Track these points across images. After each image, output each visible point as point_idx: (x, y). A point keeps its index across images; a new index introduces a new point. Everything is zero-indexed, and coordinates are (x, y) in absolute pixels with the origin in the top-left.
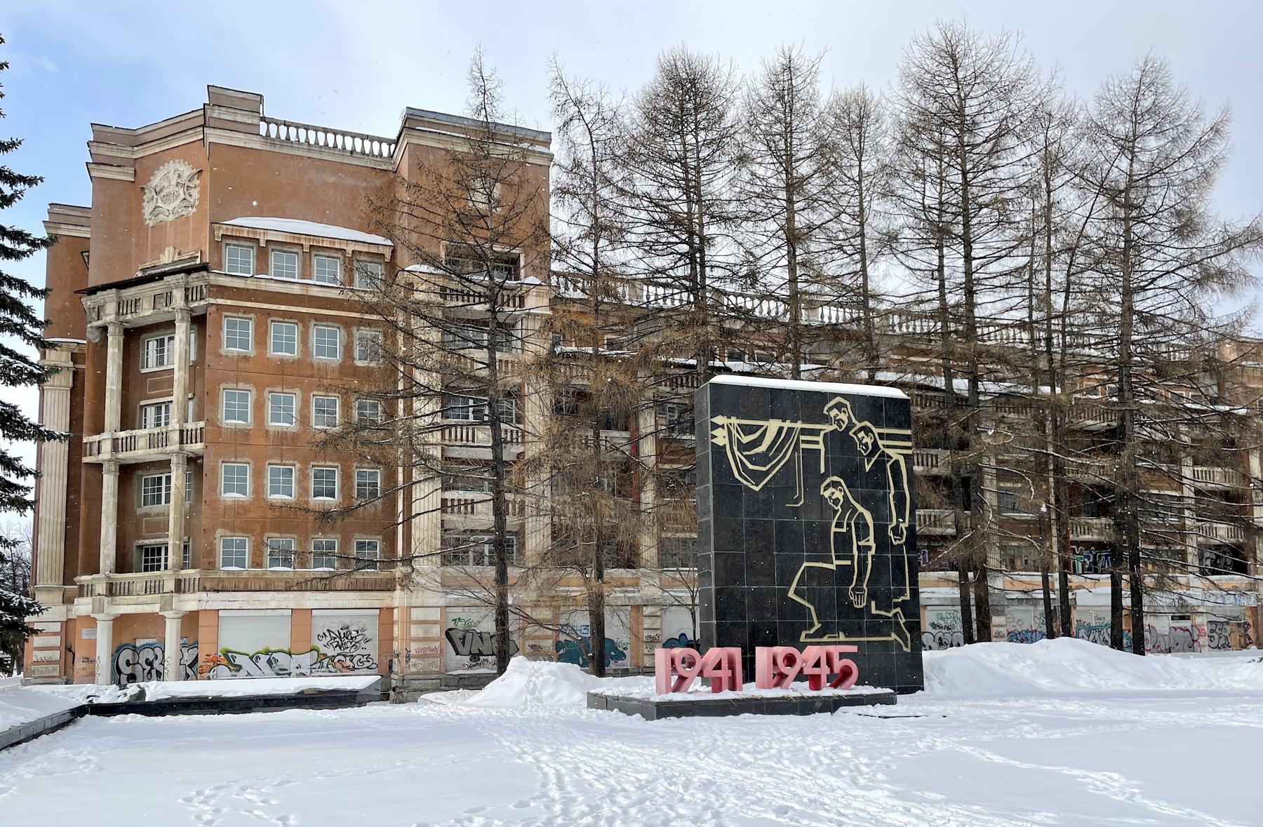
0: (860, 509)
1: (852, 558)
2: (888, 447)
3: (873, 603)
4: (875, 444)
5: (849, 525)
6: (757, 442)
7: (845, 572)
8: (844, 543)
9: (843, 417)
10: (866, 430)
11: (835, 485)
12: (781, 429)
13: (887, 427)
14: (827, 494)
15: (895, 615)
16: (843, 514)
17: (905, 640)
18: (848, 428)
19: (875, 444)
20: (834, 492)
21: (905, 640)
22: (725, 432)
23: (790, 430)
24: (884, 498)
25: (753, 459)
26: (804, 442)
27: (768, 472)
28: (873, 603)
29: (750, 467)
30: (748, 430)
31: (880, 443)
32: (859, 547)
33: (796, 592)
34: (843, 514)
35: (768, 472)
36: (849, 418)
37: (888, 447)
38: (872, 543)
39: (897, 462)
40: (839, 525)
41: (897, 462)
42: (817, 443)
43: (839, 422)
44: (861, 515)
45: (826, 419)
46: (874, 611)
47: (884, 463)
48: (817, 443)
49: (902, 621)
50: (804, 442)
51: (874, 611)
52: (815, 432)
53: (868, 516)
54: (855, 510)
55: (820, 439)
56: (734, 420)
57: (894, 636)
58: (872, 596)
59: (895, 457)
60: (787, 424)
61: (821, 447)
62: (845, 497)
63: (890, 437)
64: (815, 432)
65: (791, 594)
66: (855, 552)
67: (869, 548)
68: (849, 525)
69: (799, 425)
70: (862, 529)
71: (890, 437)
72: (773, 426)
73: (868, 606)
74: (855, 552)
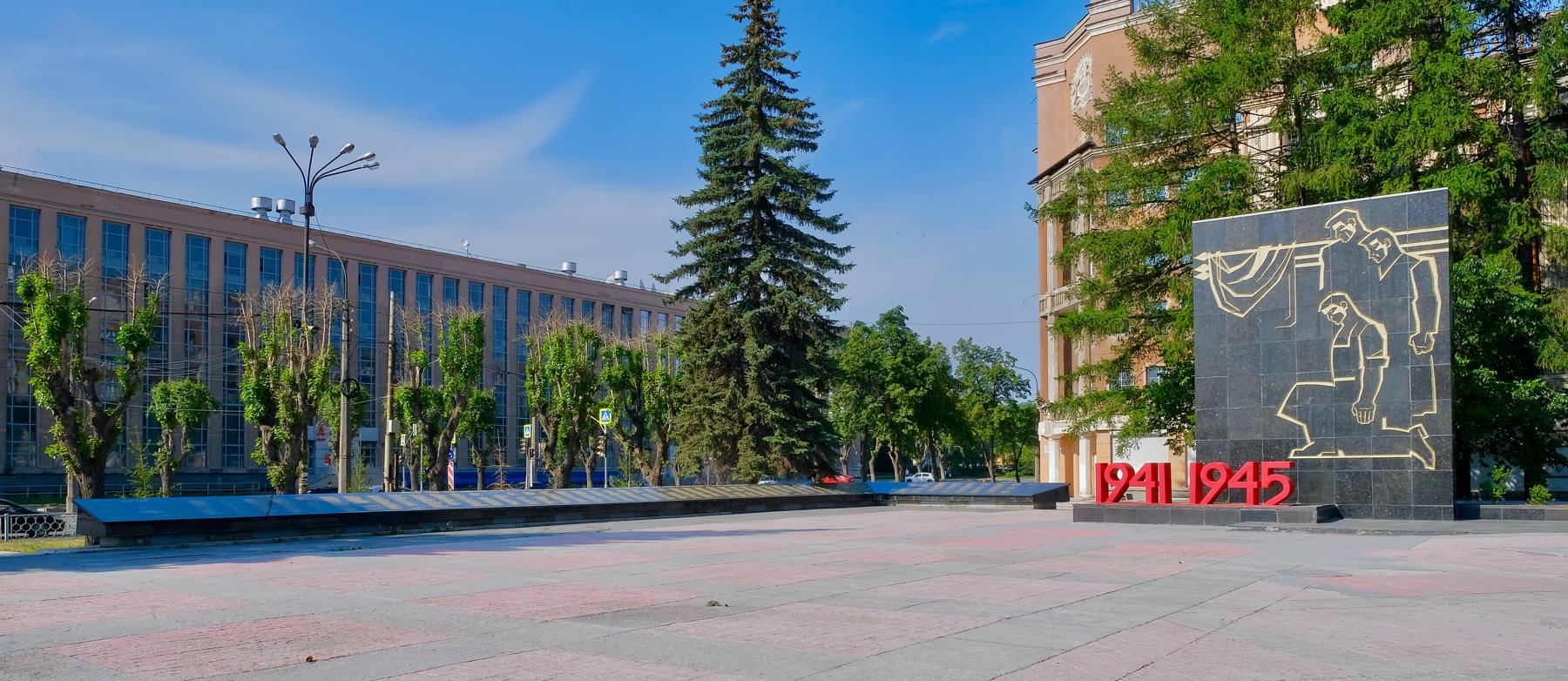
0: (1371, 322)
1: (1358, 373)
2: (1411, 249)
3: (1384, 420)
4: (1394, 250)
5: (1354, 340)
6: (1245, 270)
7: (1348, 391)
8: (1346, 360)
9: (1351, 228)
10: (1382, 237)
11: (1336, 300)
12: (1271, 254)
13: (1411, 227)
14: (1325, 311)
15: (1415, 431)
16: (1347, 329)
17: (1428, 457)
18: (1357, 237)
19: (1394, 250)
20: (1335, 309)
21: (1428, 457)
22: (1209, 267)
23: (1282, 253)
24: (1405, 306)
25: (1237, 288)
26: (1299, 262)
27: (1253, 300)
28: (1384, 420)
29: (1235, 295)
30: (1232, 261)
31: (1400, 247)
32: (1367, 363)
33: (1285, 412)
34: (1347, 329)
35: (1253, 300)
36: (1358, 227)
37: (1411, 249)
38: (1385, 355)
39: (1426, 263)
40: (1341, 340)
41: (1426, 263)
42: (1316, 260)
43: (1343, 234)
44: (1373, 328)
45: (1328, 234)
46: (1384, 427)
47: (1406, 268)
48: (1316, 260)
49: (1425, 436)
50: (1299, 262)
51: (1384, 427)
52: (1316, 249)
53: (1382, 329)
54: (1363, 323)
55: (1320, 256)
56: (1219, 254)
57: (1412, 453)
58: (1382, 411)
59: (1422, 259)
60: (1280, 247)
61: (1321, 263)
62: (1350, 311)
63: (1414, 238)
64: (1316, 249)
65: (1280, 414)
66: (1362, 366)
67: (1382, 361)
68: (1354, 340)
69: (1294, 245)
70: (1373, 341)
71: (1414, 238)
72: (1262, 252)
73: (1378, 423)
74: (1362, 366)
